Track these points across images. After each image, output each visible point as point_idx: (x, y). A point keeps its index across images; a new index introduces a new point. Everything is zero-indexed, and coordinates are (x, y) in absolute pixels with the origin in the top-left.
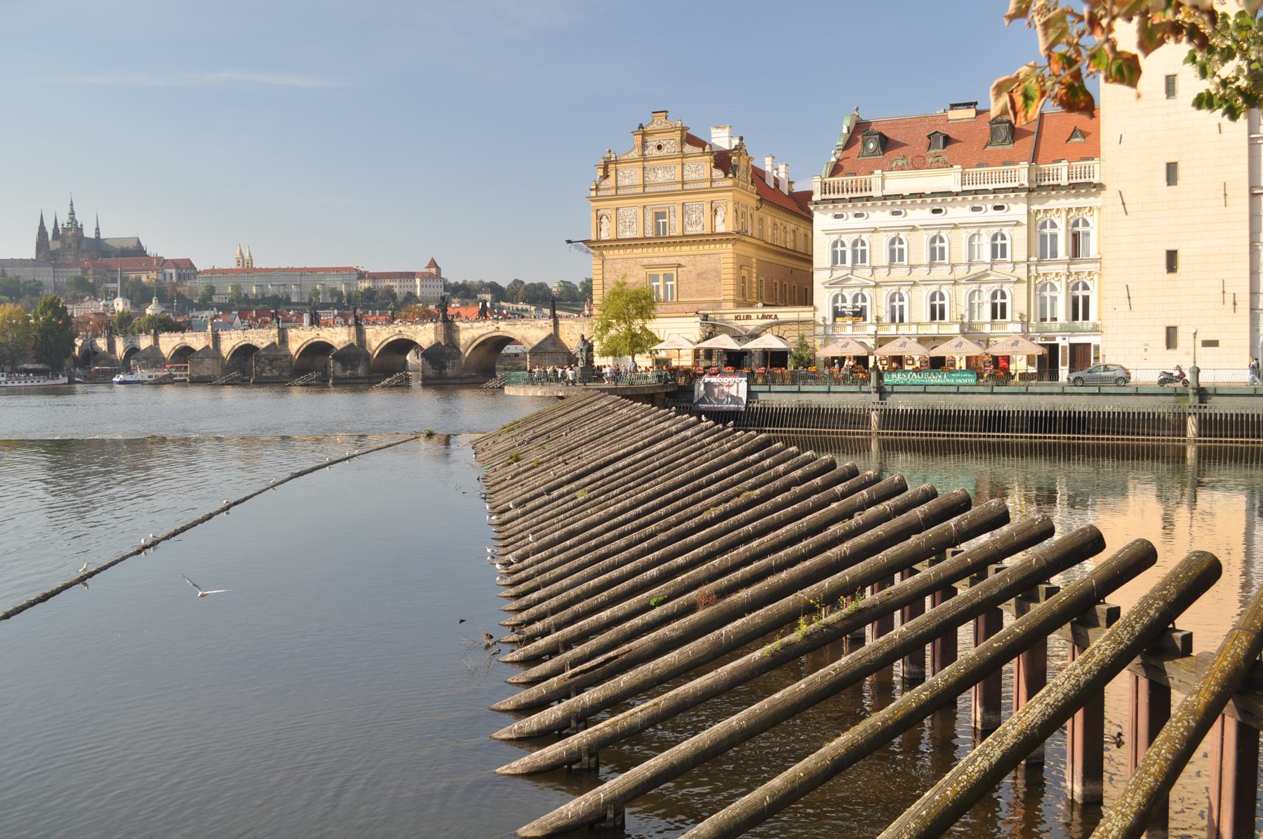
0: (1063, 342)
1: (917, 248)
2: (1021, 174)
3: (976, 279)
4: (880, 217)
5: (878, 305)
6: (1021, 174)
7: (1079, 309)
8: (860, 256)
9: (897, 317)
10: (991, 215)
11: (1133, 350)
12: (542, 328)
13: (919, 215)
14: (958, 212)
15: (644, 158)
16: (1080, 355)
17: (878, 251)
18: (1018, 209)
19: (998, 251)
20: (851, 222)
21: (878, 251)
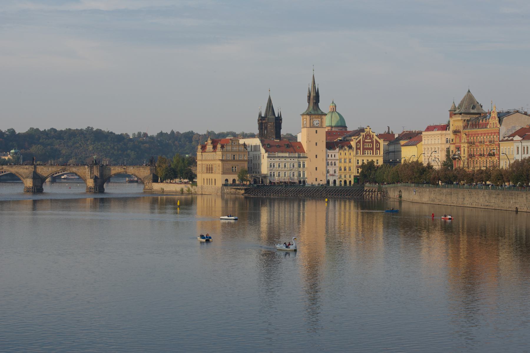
0: (302, 180)
1: (282, 165)
2: (297, 155)
3: (291, 170)
4: (277, 160)
5: (276, 174)
6: (297, 155)
7: (304, 174)
8: (274, 166)
9: (279, 175)
10: (292, 160)
11: (310, 181)
12: (26, 169)
13: (283, 160)
14: (289, 160)
15: (232, 145)
16: (304, 182)
17: (276, 165)
18: (296, 160)
19: (293, 166)
20: (272, 160)
21: (276, 165)
